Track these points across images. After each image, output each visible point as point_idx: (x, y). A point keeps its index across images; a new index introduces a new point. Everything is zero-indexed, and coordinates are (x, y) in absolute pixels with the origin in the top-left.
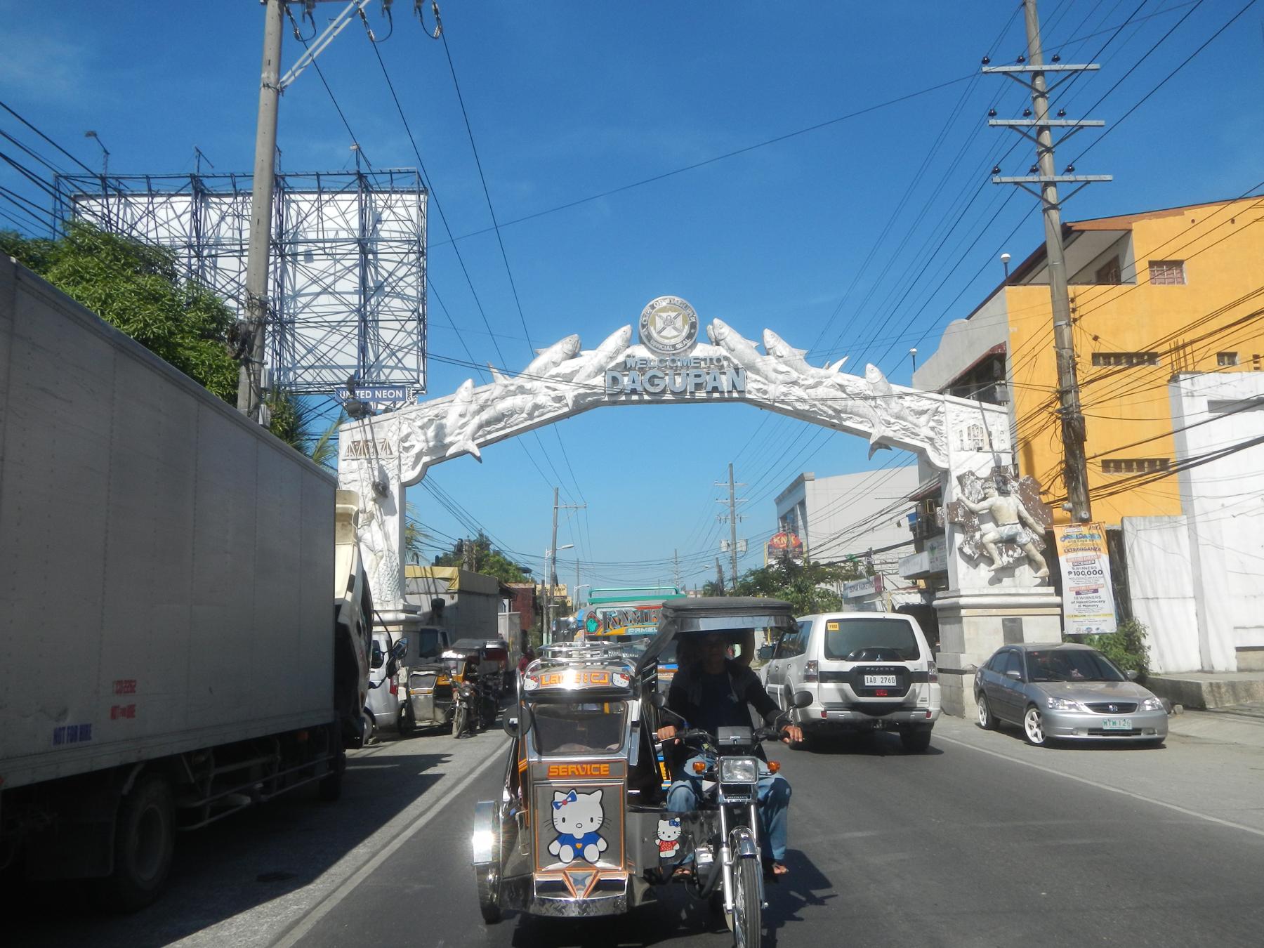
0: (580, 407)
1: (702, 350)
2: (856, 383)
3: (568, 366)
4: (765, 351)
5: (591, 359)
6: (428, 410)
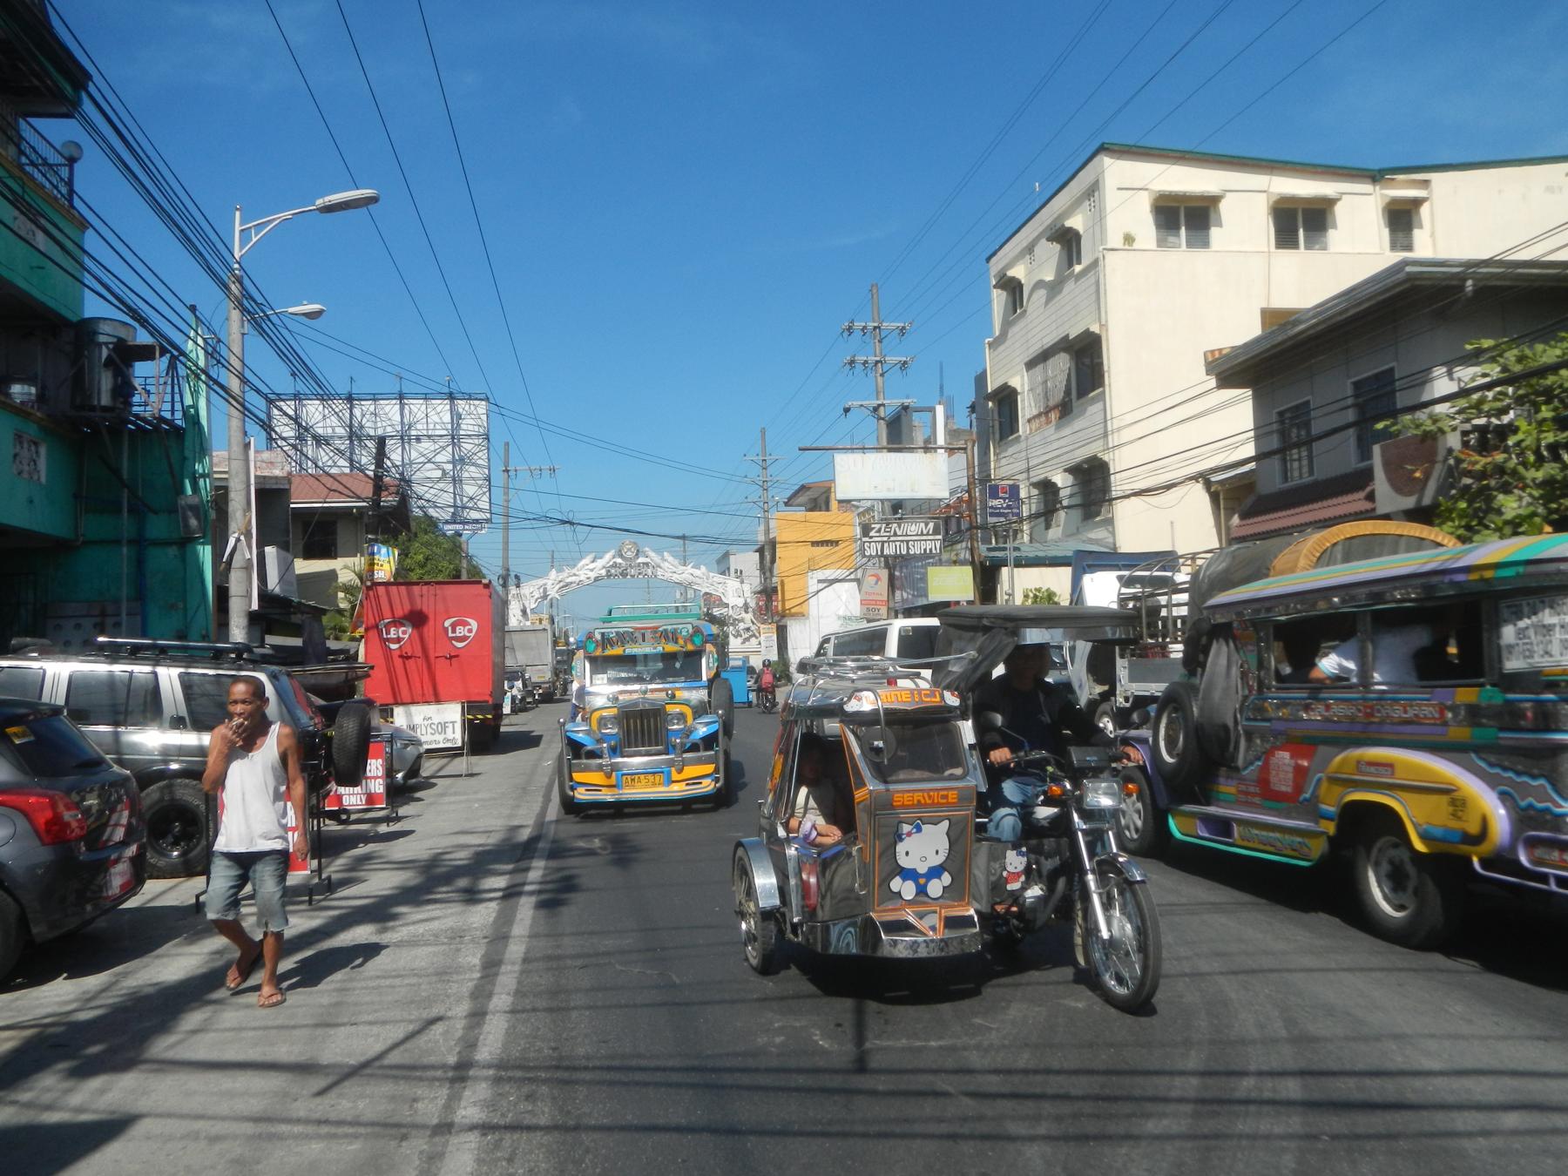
0: (596, 579)
1: (641, 560)
2: (697, 572)
3: (592, 566)
4: (664, 560)
5: (600, 563)
6: (540, 582)
